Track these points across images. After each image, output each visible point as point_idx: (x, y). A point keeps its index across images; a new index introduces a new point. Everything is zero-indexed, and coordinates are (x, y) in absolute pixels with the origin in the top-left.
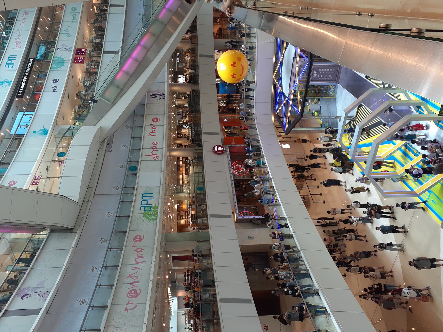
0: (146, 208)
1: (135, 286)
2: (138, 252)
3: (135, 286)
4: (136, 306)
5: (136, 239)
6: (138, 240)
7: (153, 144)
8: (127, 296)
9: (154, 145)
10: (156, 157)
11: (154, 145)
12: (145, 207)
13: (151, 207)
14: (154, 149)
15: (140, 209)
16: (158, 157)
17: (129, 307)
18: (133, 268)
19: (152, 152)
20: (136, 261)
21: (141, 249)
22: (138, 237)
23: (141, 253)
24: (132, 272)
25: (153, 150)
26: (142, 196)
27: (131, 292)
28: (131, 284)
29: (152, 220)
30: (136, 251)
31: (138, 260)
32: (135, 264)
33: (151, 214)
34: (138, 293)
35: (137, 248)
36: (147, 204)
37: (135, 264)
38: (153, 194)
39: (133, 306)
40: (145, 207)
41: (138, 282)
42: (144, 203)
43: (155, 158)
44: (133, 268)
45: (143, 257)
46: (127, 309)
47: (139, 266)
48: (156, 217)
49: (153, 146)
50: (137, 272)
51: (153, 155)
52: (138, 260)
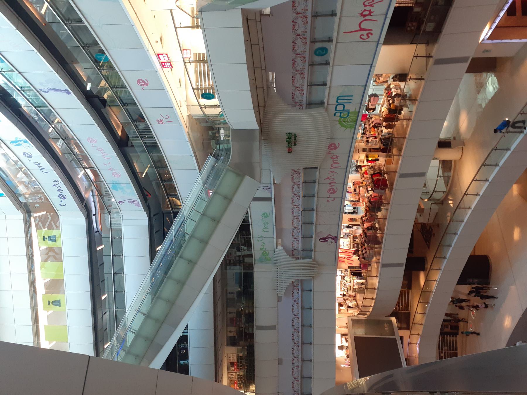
0: (342, 114)
1: (333, 186)
2: (334, 158)
3: (333, 186)
4: (334, 199)
6: (333, 147)
8: (328, 192)
10: (367, 35)
12: (341, 113)
13: (349, 113)
16: (372, 34)
17: (330, 199)
20: (332, 166)
21: (337, 156)
22: (333, 145)
24: (329, 175)
25: (362, 18)
26: (338, 99)
27: (330, 189)
28: (330, 184)
29: (349, 128)
30: (332, 158)
31: (334, 166)
32: (331, 168)
33: (349, 120)
35: (332, 155)
36: (344, 109)
37: (331, 168)
38: (353, 96)
39: (333, 199)
40: (341, 113)
41: (335, 183)
42: (340, 108)
43: (365, 37)
45: (338, 163)
46: (328, 201)
47: (336, 170)
49: (365, 10)
51: (362, 29)
52: (334, 166)
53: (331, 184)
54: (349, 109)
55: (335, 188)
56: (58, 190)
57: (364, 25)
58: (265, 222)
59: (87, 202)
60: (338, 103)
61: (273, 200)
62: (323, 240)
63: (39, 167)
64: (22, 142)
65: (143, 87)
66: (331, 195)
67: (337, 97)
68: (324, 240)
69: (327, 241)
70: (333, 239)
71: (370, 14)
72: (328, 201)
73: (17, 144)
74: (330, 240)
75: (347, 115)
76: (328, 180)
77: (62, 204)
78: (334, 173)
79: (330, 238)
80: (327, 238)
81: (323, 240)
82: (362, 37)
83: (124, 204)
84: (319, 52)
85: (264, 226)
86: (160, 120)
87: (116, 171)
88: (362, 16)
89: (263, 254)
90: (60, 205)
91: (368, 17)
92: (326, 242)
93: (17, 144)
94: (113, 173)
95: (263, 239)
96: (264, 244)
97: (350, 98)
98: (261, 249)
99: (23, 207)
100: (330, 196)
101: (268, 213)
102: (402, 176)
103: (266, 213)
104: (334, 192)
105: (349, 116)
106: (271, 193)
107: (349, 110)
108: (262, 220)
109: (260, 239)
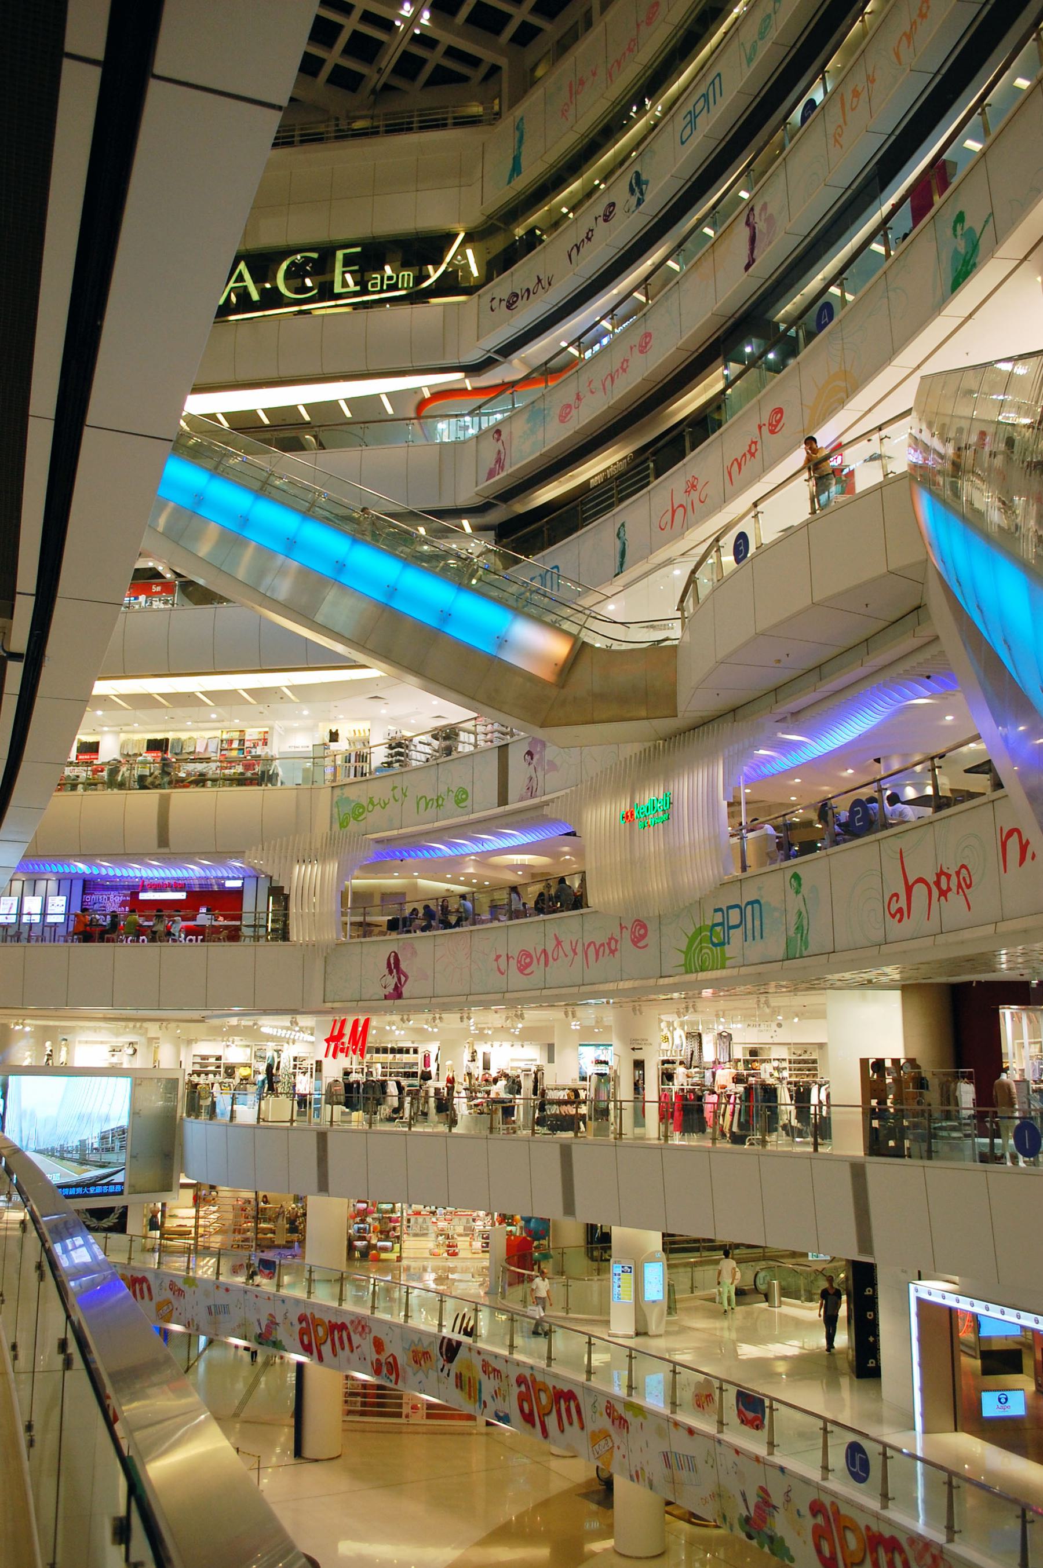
1: (538, 960)
3: (538, 960)
4: (502, 974)
5: (638, 927)
7: (958, 873)
8: (524, 950)
9: (954, 879)
10: (900, 910)
11: (954, 879)
12: (722, 924)
14: (938, 883)
15: (716, 910)
17: (503, 960)
18: (574, 944)
19: (920, 880)
21: (616, 950)
22: (642, 932)
23: (607, 951)
25: (931, 879)
27: (529, 955)
28: (544, 951)
33: (703, 951)
34: (526, 972)
38: (762, 938)
39: (503, 967)
41: (546, 964)
43: (894, 908)
44: (574, 944)
46: (498, 957)
48: (696, 968)
49: (949, 877)
50: (566, 956)
51: (909, 889)
52: (591, 951)
53: (543, 955)
54: (731, 941)
55: (534, 967)
56: (528, 290)
57: (920, 890)
58: (443, 799)
59: (503, 363)
60: (745, 908)
61: (502, 809)
62: (392, 961)
63: (583, 241)
64: (638, 194)
65: (767, 425)
66: (513, 963)
67: (759, 898)
68: (394, 965)
69: (391, 972)
70: (396, 988)
71: (943, 893)
72: (498, 957)
73: (634, 185)
74: (392, 981)
75: (715, 941)
76: (554, 942)
77: (496, 303)
78: (572, 954)
79: (399, 979)
81: (392, 961)
82: (895, 898)
83: (495, 441)
84: (858, 812)
85: (433, 799)
86: (695, 483)
87: (574, 412)
88: (937, 874)
89: (359, 805)
90: (493, 299)
91: (935, 892)
92: (387, 972)
93: (634, 185)
94: (569, 406)
95: (396, 801)
96: (385, 804)
97: (756, 934)
98: (371, 798)
99: (490, 223)
100: (511, 960)
101: (468, 803)
102: (566, 1152)
103: (466, 799)
104: (522, 969)
106: (521, 799)
107: (729, 944)
108: (449, 791)
109: (398, 793)
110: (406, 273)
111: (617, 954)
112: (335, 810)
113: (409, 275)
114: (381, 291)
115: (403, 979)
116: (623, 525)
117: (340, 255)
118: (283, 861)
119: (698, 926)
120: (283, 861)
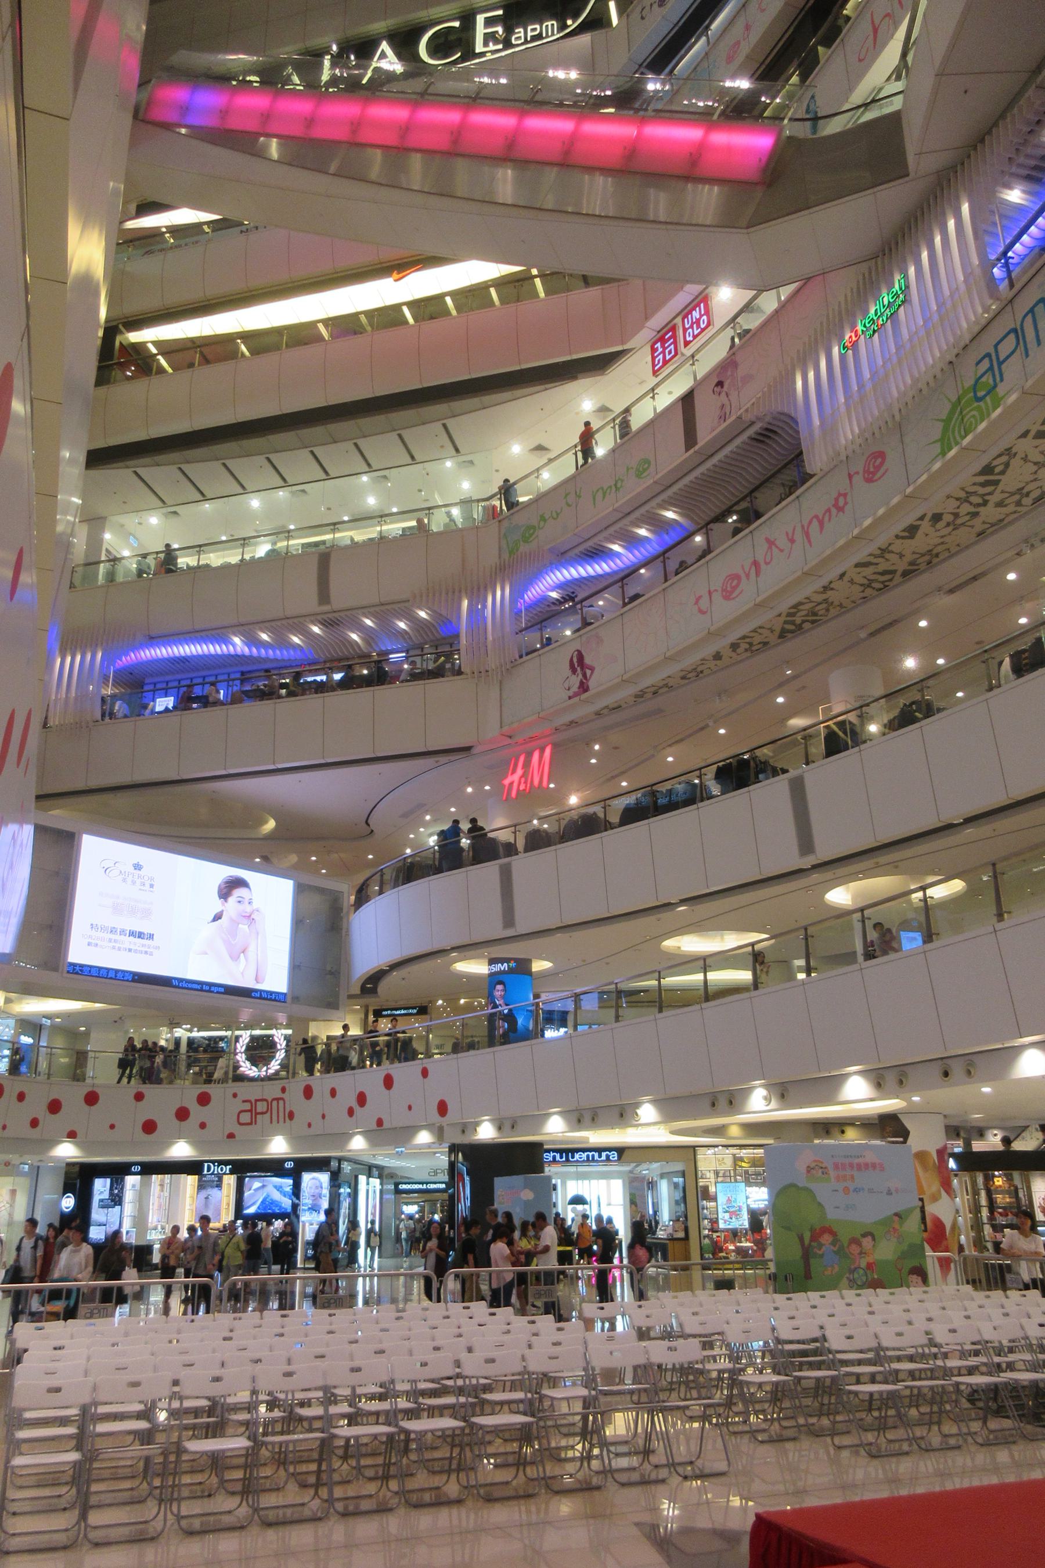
3: (748, 576)
53: (753, 568)
69: (574, 671)
70: (582, 683)
74: (575, 681)
79: (584, 675)
80: (582, 669)
92: (569, 672)
96: (558, 514)
105: (982, 404)
110: (549, 23)
111: (848, 508)
112: (504, 543)
113: (553, 25)
114: (526, 42)
115: (588, 672)
116: (813, 97)
117: (480, 19)
118: (450, 594)
119: (954, 399)
120: (450, 594)
